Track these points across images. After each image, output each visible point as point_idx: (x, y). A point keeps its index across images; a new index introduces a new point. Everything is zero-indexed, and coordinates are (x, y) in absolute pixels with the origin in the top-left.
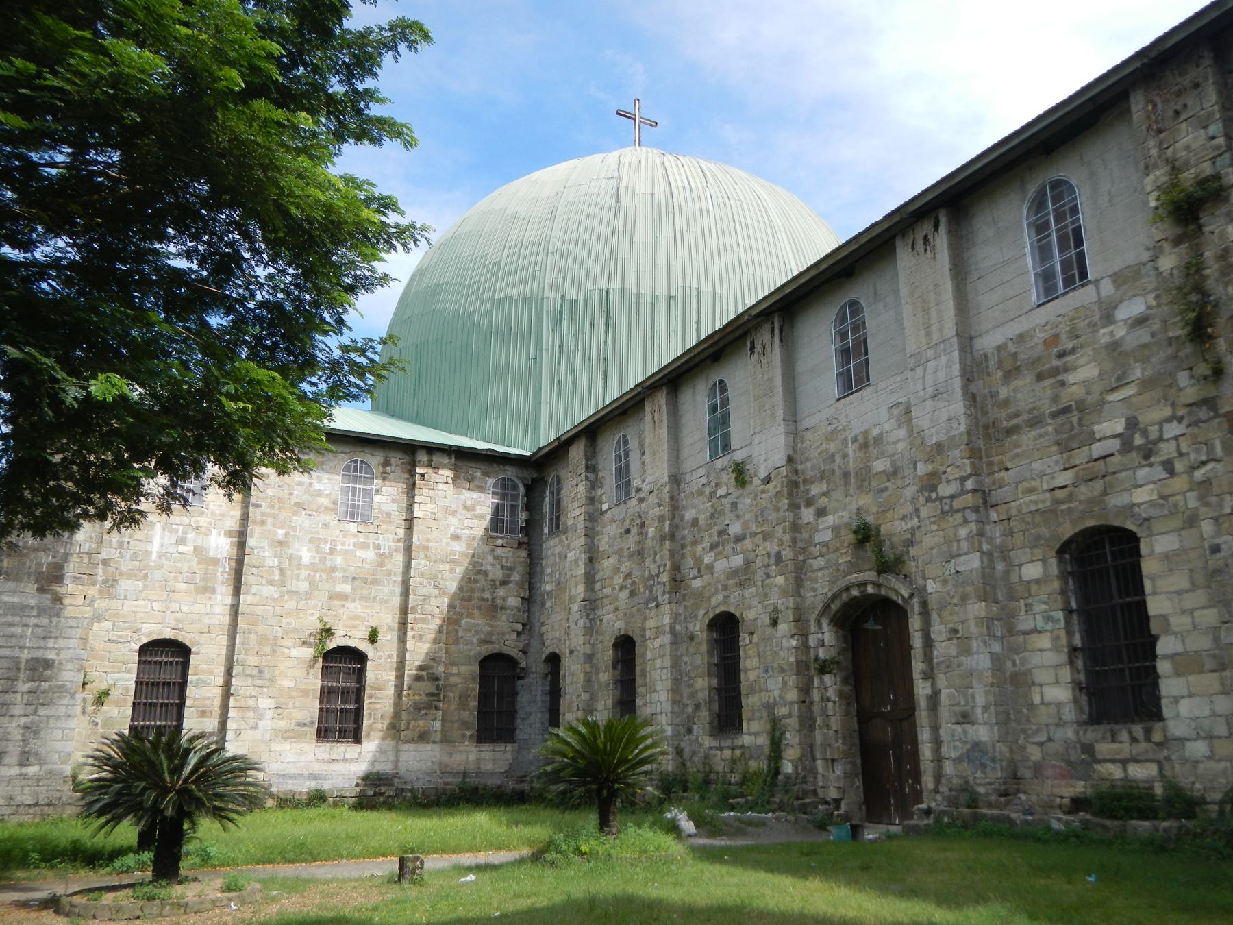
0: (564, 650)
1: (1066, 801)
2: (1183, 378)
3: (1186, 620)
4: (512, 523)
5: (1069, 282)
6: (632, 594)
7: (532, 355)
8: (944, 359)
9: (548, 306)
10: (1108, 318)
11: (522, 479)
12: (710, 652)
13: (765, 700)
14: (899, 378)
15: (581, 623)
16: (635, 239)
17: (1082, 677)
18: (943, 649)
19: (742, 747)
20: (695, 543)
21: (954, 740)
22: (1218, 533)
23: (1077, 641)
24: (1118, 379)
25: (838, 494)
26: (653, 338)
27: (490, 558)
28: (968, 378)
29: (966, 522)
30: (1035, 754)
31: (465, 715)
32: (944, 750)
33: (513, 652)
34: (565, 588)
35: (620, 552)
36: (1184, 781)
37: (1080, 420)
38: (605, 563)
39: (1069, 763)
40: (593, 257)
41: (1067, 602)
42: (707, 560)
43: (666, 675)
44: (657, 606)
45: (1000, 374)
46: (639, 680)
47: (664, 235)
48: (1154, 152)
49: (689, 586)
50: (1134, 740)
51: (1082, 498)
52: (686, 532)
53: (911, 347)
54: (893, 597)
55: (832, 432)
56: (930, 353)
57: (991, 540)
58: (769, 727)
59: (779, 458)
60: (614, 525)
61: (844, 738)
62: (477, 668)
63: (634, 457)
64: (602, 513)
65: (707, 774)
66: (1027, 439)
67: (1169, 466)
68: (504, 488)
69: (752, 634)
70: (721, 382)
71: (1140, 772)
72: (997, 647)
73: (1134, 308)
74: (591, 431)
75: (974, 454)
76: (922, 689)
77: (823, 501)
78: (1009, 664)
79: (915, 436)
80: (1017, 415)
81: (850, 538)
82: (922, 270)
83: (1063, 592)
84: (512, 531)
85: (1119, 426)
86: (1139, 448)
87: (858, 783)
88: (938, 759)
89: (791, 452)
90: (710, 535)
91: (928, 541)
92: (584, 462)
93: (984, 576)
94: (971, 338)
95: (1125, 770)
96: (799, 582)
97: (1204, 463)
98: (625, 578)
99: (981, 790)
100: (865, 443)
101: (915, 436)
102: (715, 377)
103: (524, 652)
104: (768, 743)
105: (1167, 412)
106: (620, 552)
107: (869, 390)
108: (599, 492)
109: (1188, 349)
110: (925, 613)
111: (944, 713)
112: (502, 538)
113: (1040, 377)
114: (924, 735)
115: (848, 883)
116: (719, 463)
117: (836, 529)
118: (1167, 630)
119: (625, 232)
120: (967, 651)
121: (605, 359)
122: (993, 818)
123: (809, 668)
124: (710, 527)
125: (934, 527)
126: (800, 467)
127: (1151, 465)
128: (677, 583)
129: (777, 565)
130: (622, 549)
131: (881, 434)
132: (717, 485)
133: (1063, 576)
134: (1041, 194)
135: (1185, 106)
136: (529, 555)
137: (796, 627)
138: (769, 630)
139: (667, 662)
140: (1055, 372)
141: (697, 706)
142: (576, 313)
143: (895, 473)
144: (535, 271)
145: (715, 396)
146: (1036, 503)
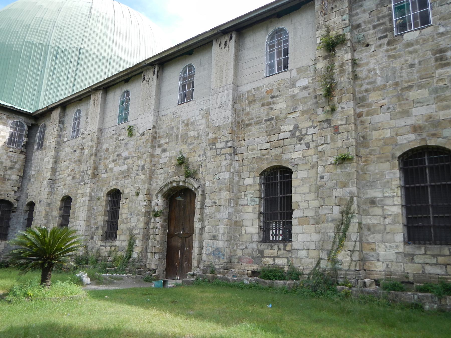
0: (37, 201)
1: (250, 272)
2: (319, 111)
3: (306, 204)
4: (19, 142)
5: (279, 69)
6: (73, 178)
7: (40, 69)
8: (226, 93)
9: (51, 50)
10: (293, 85)
11: (27, 124)
12: (106, 206)
13: (129, 226)
14: (205, 99)
15: (47, 189)
16: (96, 30)
17: (262, 224)
18: (208, 210)
19: (115, 246)
20: (106, 158)
21: (208, 246)
22: (324, 172)
23: (262, 210)
24: (293, 109)
25: (173, 144)
26: (98, 74)
27: (5, 156)
29: (226, 159)
30: (239, 253)
32: (204, 251)
33: (12, 200)
34: (42, 173)
35: (70, 160)
36: (296, 266)
37: (276, 123)
38: (62, 164)
39: (253, 257)
40: (76, 33)
41: (261, 195)
43: (84, 214)
44: (84, 184)
45: (247, 102)
47: (109, 31)
48: (322, 22)
49: (101, 177)
50: (279, 249)
51: (273, 154)
52: (102, 154)
53: (213, 86)
54: (191, 187)
55: (174, 118)
56: (221, 89)
57: (234, 168)
58: (129, 238)
59: (150, 126)
60: (69, 148)
61: (161, 244)
63: (83, 119)
64: (64, 142)
65: (98, 257)
66: (254, 129)
68: (17, 126)
69: (127, 199)
70: (128, 91)
71: (279, 262)
72: (231, 210)
73: (303, 82)
74: (64, 106)
75: (233, 132)
76: (197, 225)
77: (165, 146)
78: (234, 217)
79: (209, 122)
80: (252, 119)
81: (176, 162)
82: (222, 55)
83: (260, 190)
84: (18, 146)
85: (291, 128)
86: (297, 137)
87: (164, 262)
88: (200, 254)
89: (155, 124)
90: (113, 156)
91: (209, 165)
92: (58, 118)
93: (230, 182)
94: (238, 86)
95: (274, 261)
96: (151, 179)
97: (322, 144)
98: (71, 171)
99: (217, 267)
101: (209, 122)
102: (126, 88)
103: (17, 200)
104: (128, 245)
105: (310, 124)
106: (70, 160)
107: (192, 102)
108: (64, 133)
109: (323, 100)
110: (203, 195)
111: (206, 236)
112: (13, 148)
113: (263, 105)
114: (196, 244)
115: (171, 311)
116: (122, 126)
117: (170, 158)
118: (298, 207)
119: (92, 26)
120: (219, 211)
121: (75, 78)
122: (221, 278)
123: (151, 214)
124: (114, 152)
125: (212, 160)
126: (157, 131)
127: (301, 144)
128: (95, 175)
129: (142, 170)
130: (71, 158)
131: (195, 120)
132: (119, 135)
133: (261, 184)
134: (274, 34)
135: (336, 6)
136: (26, 158)
137: (147, 197)
138: (135, 197)
139: (86, 208)
140: (270, 104)
141: (97, 228)
142: (64, 55)
144: (46, 32)
145: (124, 97)
146: (254, 154)
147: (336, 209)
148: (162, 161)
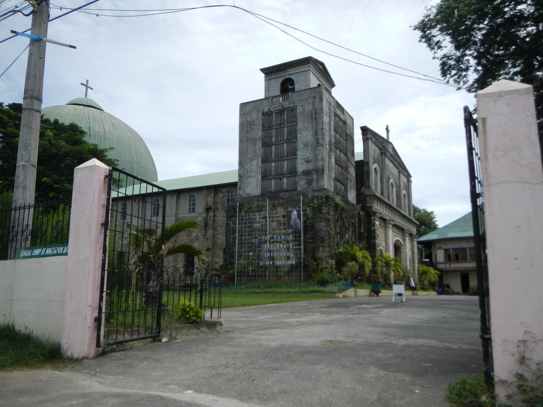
10: (197, 219)
73: (200, 219)
85: (195, 235)
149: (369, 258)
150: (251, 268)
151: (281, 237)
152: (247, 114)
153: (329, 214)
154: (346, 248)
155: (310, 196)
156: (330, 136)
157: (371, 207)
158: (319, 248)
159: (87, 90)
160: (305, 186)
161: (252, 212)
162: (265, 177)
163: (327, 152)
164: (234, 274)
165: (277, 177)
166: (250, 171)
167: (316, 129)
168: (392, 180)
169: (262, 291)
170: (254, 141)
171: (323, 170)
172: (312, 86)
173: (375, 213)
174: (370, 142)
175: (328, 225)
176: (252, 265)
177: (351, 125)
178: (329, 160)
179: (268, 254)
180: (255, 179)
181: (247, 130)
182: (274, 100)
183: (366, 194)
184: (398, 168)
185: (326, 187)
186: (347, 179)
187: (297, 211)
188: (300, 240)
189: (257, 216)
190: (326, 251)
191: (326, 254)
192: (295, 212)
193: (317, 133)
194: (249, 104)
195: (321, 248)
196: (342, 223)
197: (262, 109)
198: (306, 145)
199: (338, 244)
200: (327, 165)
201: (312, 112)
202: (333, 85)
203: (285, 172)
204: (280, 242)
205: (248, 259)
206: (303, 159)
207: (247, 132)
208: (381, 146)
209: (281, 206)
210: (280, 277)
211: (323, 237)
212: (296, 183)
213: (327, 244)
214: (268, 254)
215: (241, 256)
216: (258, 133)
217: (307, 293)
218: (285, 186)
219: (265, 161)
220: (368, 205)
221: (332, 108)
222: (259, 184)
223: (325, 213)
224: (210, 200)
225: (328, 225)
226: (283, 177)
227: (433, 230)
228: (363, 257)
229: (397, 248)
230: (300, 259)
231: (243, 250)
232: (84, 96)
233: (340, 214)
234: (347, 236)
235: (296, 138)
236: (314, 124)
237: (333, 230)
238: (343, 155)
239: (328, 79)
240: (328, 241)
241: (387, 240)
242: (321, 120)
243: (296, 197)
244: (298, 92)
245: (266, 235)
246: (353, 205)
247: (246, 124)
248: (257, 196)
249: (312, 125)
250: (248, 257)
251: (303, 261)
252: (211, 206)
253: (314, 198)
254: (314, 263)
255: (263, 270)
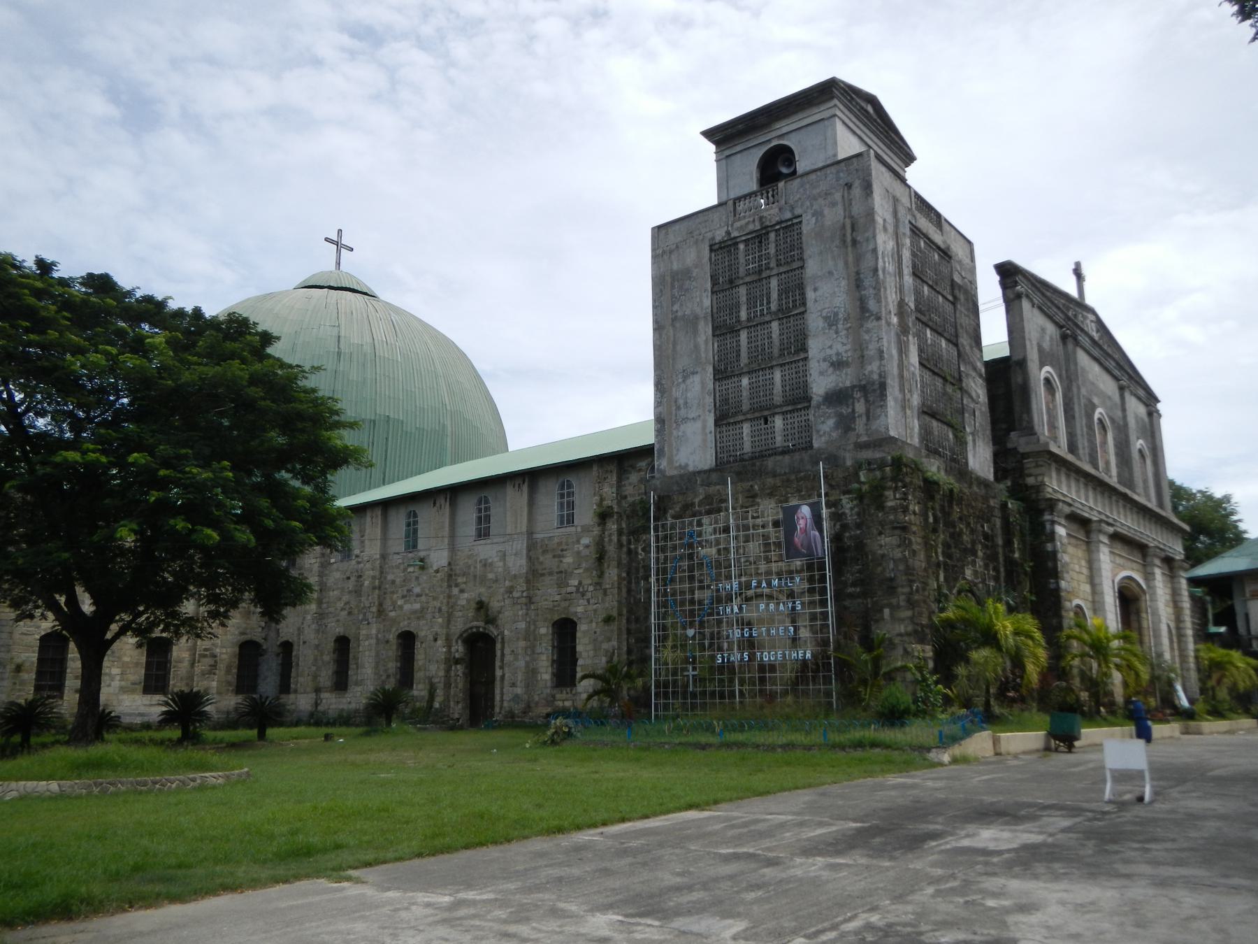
6: (350, 613)
10: (578, 542)
18: (508, 658)
20: (393, 593)
21: (509, 693)
28: (529, 550)
30: (536, 698)
31: (229, 678)
35: (343, 589)
42: (399, 603)
46: (351, 661)
53: (509, 531)
59: (444, 562)
62: (237, 650)
66: (547, 579)
67: (588, 601)
71: (568, 704)
72: (528, 658)
73: (585, 541)
75: (528, 581)
76: (498, 673)
81: (474, 605)
82: (516, 499)
88: (502, 701)
96: (449, 622)
100: (485, 564)
103: (265, 639)
110: (503, 642)
111: (506, 683)
113: (554, 557)
114: (497, 691)
117: (468, 601)
123: (451, 661)
128: (381, 612)
133: (553, 634)
140: (559, 556)
141: (388, 676)
143: (496, 581)
147: (604, 659)
148: (460, 602)
149: (1038, 635)
150: (691, 673)
151: (769, 584)
152: (671, 252)
153: (905, 510)
154: (963, 608)
155: (849, 463)
156: (901, 289)
157: (1039, 488)
158: (881, 611)
159: (339, 252)
160: (834, 435)
161: (694, 515)
162: (725, 417)
163: (893, 334)
164: (647, 689)
165: (757, 415)
166: (686, 403)
167: (858, 273)
168: (1099, 410)
169: (714, 740)
170: (692, 323)
171: (883, 386)
172: (841, 156)
173: (1052, 504)
174: (1026, 304)
175: (905, 543)
176: (694, 662)
177: (967, 261)
178: (901, 361)
179: (737, 633)
180: (698, 424)
181: (673, 296)
182: (741, 206)
183: (1021, 450)
184: (1116, 379)
185: (892, 433)
186: (962, 411)
187: (810, 505)
188: (823, 591)
189: (708, 526)
190: (902, 620)
191: (902, 629)
192: (805, 510)
193: (862, 284)
194: (677, 227)
195: (887, 611)
196: (952, 535)
197: (709, 235)
198: (831, 321)
199: (941, 598)
200: (895, 371)
201: (844, 227)
202: (909, 158)
203: (778, 399)
204: (770, 597)
205: (684, 647)
206: (825, 360)
207: (674, 300)
208: (1060, 318)
209: (771, 495)
210: (772, 697)
211: (891, 580)
212: (808, 428)
213: (902, 598)
214: (737, 633)
215: (665, 638)
216: (702, 300)
217: (842, 747)
218: (779, 440)
219: (721, 374)
220: (1030, 481)
221: (902, 212)
222: (711, 438)
223: (894, 509)
224: (609, 491)
225: (905, 543)
226: (773, 415)
227: (1232, 547)
228: (1017, 633)
229: (1129, 600)
230: (825, 643)
231: (669, 621)
232: (332, 267)
233: (942, 508)
234: (968, 573)
235: (804, 304)
236: (851, 259)
237: (922, 556)
238: (944, 343)
239: (893, 142)
240: (906, 590)
241: (1097, 581)
242: (871, 246)
243: (809, 467)
244: (802, 176)
245: (729, 577)
246: (983, 483)
247: (668, 279)
248: (705, 472)
249: (846, 263)
250: (682, 644)
251: (836, 650)
252: (611, 507)
253: (858, 466)
254: (864, 657)
255: (725, 677)
